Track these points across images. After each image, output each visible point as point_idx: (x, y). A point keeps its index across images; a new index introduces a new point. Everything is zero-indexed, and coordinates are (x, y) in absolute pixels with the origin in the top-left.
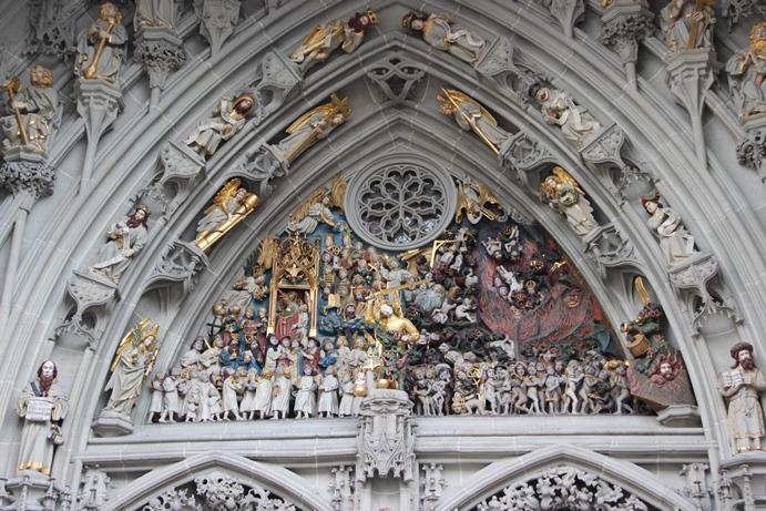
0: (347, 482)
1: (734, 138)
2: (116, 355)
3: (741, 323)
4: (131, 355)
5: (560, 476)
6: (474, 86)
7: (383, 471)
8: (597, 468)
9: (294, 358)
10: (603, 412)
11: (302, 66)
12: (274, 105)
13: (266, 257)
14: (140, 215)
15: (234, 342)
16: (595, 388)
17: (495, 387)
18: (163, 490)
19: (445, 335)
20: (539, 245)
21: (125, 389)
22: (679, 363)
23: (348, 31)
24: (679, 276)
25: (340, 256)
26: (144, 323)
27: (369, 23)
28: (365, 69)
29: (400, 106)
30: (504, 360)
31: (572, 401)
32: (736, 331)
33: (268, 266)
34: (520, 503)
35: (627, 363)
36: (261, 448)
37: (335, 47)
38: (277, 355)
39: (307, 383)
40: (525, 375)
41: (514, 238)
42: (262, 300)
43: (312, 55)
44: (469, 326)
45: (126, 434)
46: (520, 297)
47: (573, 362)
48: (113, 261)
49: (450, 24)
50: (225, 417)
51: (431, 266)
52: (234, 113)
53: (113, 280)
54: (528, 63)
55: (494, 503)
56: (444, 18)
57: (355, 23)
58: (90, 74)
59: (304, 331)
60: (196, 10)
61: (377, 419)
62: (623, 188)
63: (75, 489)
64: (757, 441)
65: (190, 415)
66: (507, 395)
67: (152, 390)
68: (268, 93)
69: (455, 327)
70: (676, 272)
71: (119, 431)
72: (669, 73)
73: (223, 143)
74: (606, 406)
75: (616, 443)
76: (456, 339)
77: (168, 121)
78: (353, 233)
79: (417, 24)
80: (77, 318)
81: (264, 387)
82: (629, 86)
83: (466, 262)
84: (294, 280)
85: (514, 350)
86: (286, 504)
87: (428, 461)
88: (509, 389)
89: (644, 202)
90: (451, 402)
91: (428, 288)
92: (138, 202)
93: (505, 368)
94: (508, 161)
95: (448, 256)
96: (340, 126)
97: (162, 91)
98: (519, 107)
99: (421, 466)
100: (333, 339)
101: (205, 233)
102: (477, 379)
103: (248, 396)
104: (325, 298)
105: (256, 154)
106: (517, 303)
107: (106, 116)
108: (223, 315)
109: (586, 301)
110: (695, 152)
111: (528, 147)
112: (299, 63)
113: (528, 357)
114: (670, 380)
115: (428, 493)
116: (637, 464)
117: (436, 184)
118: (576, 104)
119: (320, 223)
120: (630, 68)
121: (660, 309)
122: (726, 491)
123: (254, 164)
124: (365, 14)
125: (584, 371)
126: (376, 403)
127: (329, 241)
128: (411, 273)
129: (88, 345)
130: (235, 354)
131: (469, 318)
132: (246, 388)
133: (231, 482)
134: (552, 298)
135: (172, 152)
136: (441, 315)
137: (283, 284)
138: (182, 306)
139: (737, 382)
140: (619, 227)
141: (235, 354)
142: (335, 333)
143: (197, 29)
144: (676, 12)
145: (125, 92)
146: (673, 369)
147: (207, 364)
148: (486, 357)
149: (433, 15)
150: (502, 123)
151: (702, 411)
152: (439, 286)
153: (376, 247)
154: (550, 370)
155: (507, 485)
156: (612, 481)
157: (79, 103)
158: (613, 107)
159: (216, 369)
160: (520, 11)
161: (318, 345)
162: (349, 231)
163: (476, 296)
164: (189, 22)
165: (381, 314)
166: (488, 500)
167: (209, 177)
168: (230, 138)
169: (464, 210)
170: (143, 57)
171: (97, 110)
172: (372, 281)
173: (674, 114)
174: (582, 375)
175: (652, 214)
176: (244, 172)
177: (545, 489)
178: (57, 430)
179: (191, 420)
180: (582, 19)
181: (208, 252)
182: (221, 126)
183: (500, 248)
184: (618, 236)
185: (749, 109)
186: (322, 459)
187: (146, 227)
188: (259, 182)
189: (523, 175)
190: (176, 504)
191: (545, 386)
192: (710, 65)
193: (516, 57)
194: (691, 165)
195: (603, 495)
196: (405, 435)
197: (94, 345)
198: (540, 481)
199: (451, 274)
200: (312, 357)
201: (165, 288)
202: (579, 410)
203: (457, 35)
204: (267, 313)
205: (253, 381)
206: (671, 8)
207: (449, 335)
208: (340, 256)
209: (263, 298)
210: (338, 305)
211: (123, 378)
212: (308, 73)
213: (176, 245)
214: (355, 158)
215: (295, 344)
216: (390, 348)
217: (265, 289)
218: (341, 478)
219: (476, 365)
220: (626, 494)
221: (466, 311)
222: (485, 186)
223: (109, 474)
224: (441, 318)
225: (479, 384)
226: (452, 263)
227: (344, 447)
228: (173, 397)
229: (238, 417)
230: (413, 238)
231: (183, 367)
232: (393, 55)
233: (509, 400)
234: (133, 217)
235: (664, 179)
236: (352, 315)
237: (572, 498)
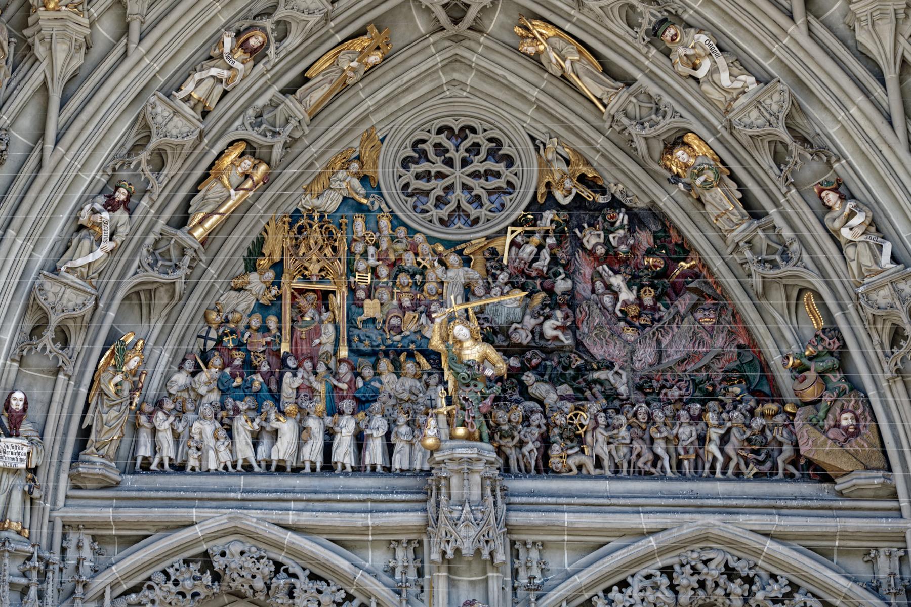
6: (568, 18)
9: (320, 387)
15: (238, 362)
38: (298, 382)
69: (543, 350)
83: (554, 260)
106: (625, 316)
136: (521, 331)
147: (203, 390)
150: (608, 69)
152: (520, 294)
161: (353, 369)
163: (570, 307)
171: (61, 51)
181: (203, 243)
200: (344, 387)
215: (321, 369)
221: (556, 328)
224: (522, 337)
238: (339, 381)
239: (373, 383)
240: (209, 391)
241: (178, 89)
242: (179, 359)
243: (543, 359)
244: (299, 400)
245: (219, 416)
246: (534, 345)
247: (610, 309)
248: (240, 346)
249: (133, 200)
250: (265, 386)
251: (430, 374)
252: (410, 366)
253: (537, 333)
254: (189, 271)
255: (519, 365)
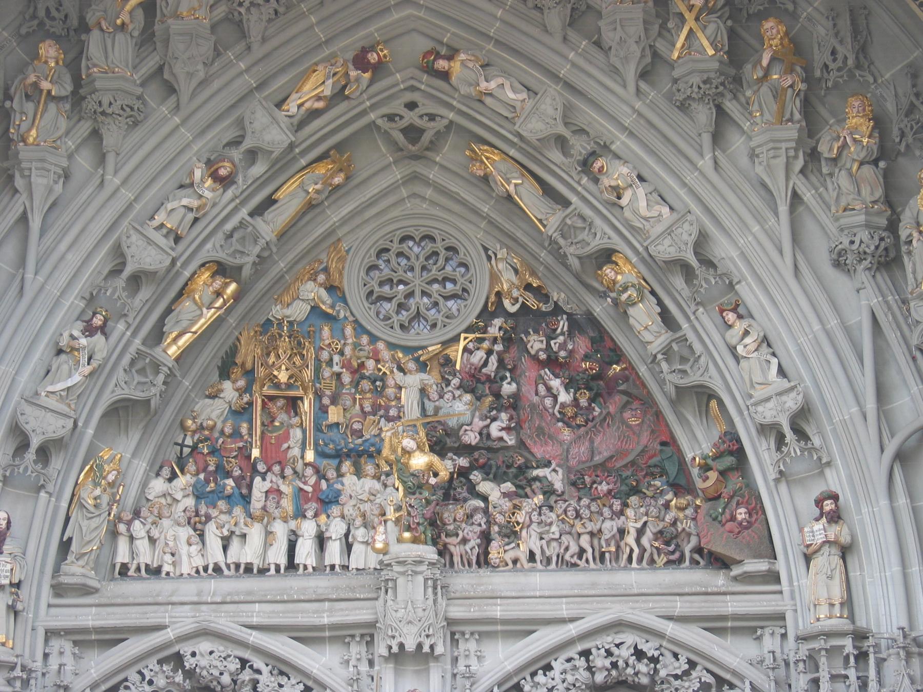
0: (364, 654)
1: (829, 238)
2: (73, 495)
3: (829, 464)
4: (92, 496)
5: (618, 646)
7: (410, 646)
8: (660, 635)
10: (669, 563)
11: (295, 121)
12: (258, 169)
13: (246, 355)
14: (98, 321)
15: (212, 468)
16: (659, 534)
17: (541, 533)
18: (143, 663)
19: (477, 460)
20: (593, 341)
21: (87, 539)
22: (757, 508)
23: (353, 73)
24: (760, 409)
25: (342, 353)
26: (106, 454)
27: (380, 61)
28: (372, 116)
29: (416, 157)
30: (549, 491)
31: (632, 551)
32: (822, 473)
33: (249, 366)
34: (570, 678)
35: (698, 502)
36: (259, 614)
37: (336, 91)
38: (267, 485)
39: (308, 528)
40: (576, 518)
41: (562, 333)
42: (242, 412)
43: (307, 105)
44: (507, 448)
45: (92, 593)
46: (570, 412)
47: (633, 500)
48: (69, 383)
49: (481, 66)
50: (210, 571)
51: (458, 367)
52: (209, 182)
53: (69, 406)
54: (582, 122)
55: (540, 678)
56: (477, 59)
57: (360, 62)
58: (31, 140)
59: (296, 452)
60: (159, 45)
61: (401, 581)
62: (697, 291)
63: (38, 664)
64: (837, 607)
65: (166, 568)
66: (554, 544)
67: (114, 534)
68: (252, 155)
69: (489, 449)
70: (756, 404)
71: (86, 590)
72: (753, 150)
73: (196, 220)
74: (672, 557)
75: (680, 606)
76: (491, 467)
77: (127, 195)
78: (356, 321)
79: (442, 64)
80: (31, 455)
81: (255, 533)
82: (705, 163)
84: (283, 386)
85: (563, 480)
86: (293, 681)
87: (462, 628)
88: (557, 536)
89: (722, 311)
90: (487, 553)
91: (454, 398)
92: (91, 300)
93: (551, 508)
94: (557, 243)
95: (479, 356)
96: (338, 187)
97: (118, 154)
98: (572, 178)
99: (453, 634)
100: (334, 462)
101: (174, 335)
102: (518, 523)
103: (235, 543)
104: (324, 410)
105: (235, 229)
107: (51, 191)
108: (194, 432)
109: (650, 417)
110: (781, 252)
111: (580, 224)
112: (290, 117)
113: (579, 489)
114: (746, 528)
115: (461, 668)
116: (705, 629)
117: (461, 255)
118: (641, 178)
119: (312, 307)
120: (707, 139)
121: (739, 441)
122: (801, 665)
123: (235, 244)
124: (372, 48)
125: (647, 514)
126: (399, 563)
127: (326, 331)
128: (430, 379)
129: (43, 486)
130: (212, 485)
131: (506, 437)
132: (232, 533)
133: (223, 655)
134: (609, 413)
135: (135, 237)
137: (267, 391)
138: (146, 427)
139: (820, 539)
140: (691, 337)
141: (212, 485)
142: (339, 456)
143: (160, 69)
144: (759, 73)
145: (70, 157)
146: (750, 515)
147: (179, 496)
148: (528, 490)
149: (462, 56)
150: (548, 191)
151: (781, 566)
152: (468, 397)
153: (385, 341)
154: (606, 512)
155: (555, 656)
156: (677, 650)
157: (17, 175)
158: (684, 185)
159: (190, 502)
160: (572, 55)
161: (317, 471)
162: (351, 319)
164: (152, 63)
165: (403, 449)
166: (534, 674)
167: (179, 264)
168: (204, 215)
169: (499, 294)
170: (95, 112)
171: (39, 182)
172: (384, 387)
173: (757, 202)
174: (645, 519)
175: (730, 326)
176: (222, 256)
177: (600, 661)
178: (17, 594)
179: (168, 574)
180: (649, 68)
181: (178, 359)
182: (195, 203)
183: (544, 346)
184: (690, 347)
185: (843, 204)
186: (334, 627)
187: (104, 333)
188: (240, 268)
189: (574, 263)
190: (161, 682)
191: (600, 531)
192: (799, 141)
193: (568, 113)
194: (775, 266)
195: (665, 666)
196: (435, 601)
197: (50, 487)
198: (594, 651)
199: (483, 379)
200: (309, 489)
201: (128, 407)
202: (640, 560)
203: (493, 85)
204: (250, 429)
205: (242, 525)
206: (754, 67)
207: (481, 461)
208: (342, 353)
209: (244, 409)
210: (341, 420)
211: (85, 523)
212: (301, 125)
213: (139, 352)
214: (357, 221)
216: (414, 493)
217: (246, 398)
218: (357, 650)
219: (516, 501)
220: (692, 664)
221: (503, 429)
222: (523, 262)
223: (76, 643)
224: (471, 438)
225: (521, 529)
226: (486, 364)
227: (360, 614)
228: (143, 545)
229: (226, 572)
230: (434, 326)
231: (148, 500)
232: (409, 97)
233: (557, 551)
234: (89, 322)
235: (746, 279)
236: (359, 434)
237: (630, 671)
238: (305, 483)
239: (335, 486)
240: (184, 497)
241: (152, 218)
242: (157, 467)
243: (489, 459)
244: (268, 502)
245: (192, 521)
246: (481, 445)
247: (551, 411)
248: (213, 452)
249: (110, 323)
250: (237, 491)
251: (388, 475)
252: (370, 469)
253: (484, 434)
254: (163, 388)
255: (467, 465)
